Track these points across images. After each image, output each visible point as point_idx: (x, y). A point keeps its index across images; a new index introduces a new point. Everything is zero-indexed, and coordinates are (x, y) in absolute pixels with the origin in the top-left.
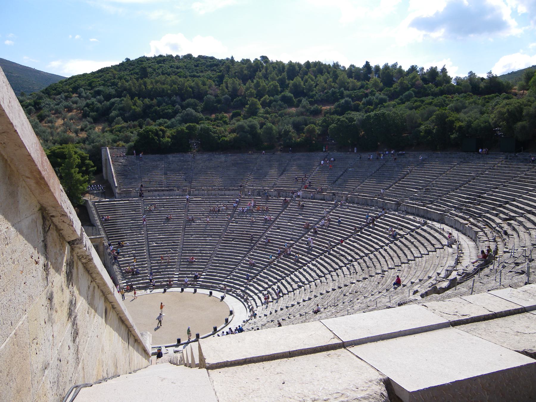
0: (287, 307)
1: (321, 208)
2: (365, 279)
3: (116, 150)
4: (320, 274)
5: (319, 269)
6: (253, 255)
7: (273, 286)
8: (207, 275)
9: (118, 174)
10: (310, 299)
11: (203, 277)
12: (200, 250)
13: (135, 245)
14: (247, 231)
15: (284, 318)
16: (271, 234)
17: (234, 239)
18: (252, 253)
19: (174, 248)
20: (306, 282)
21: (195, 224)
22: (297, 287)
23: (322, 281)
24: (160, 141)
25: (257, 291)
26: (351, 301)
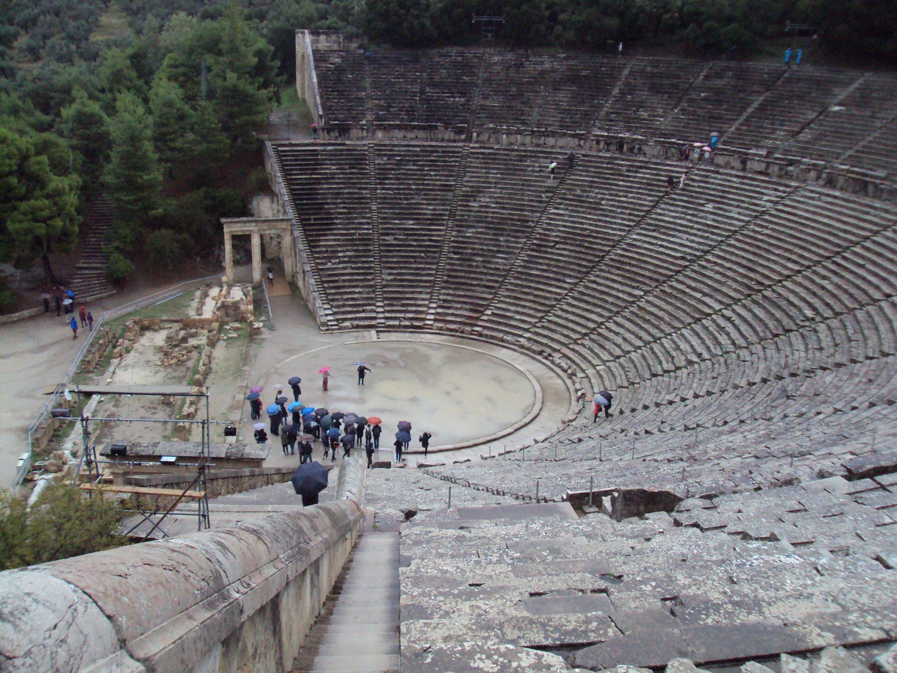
0: (658, 405)
2: (839, 365)
4: (741, 342)
5: (736, 327)
6: (594, 282)
7: (633, 355)
8: (493, 314)
10: (709, 393)
15: (648, 429)
17: (557, 243)
18: (593, 278)
19: (429, 252)
20: (706, 355)
22: (683, 363)
23: (742, 358)
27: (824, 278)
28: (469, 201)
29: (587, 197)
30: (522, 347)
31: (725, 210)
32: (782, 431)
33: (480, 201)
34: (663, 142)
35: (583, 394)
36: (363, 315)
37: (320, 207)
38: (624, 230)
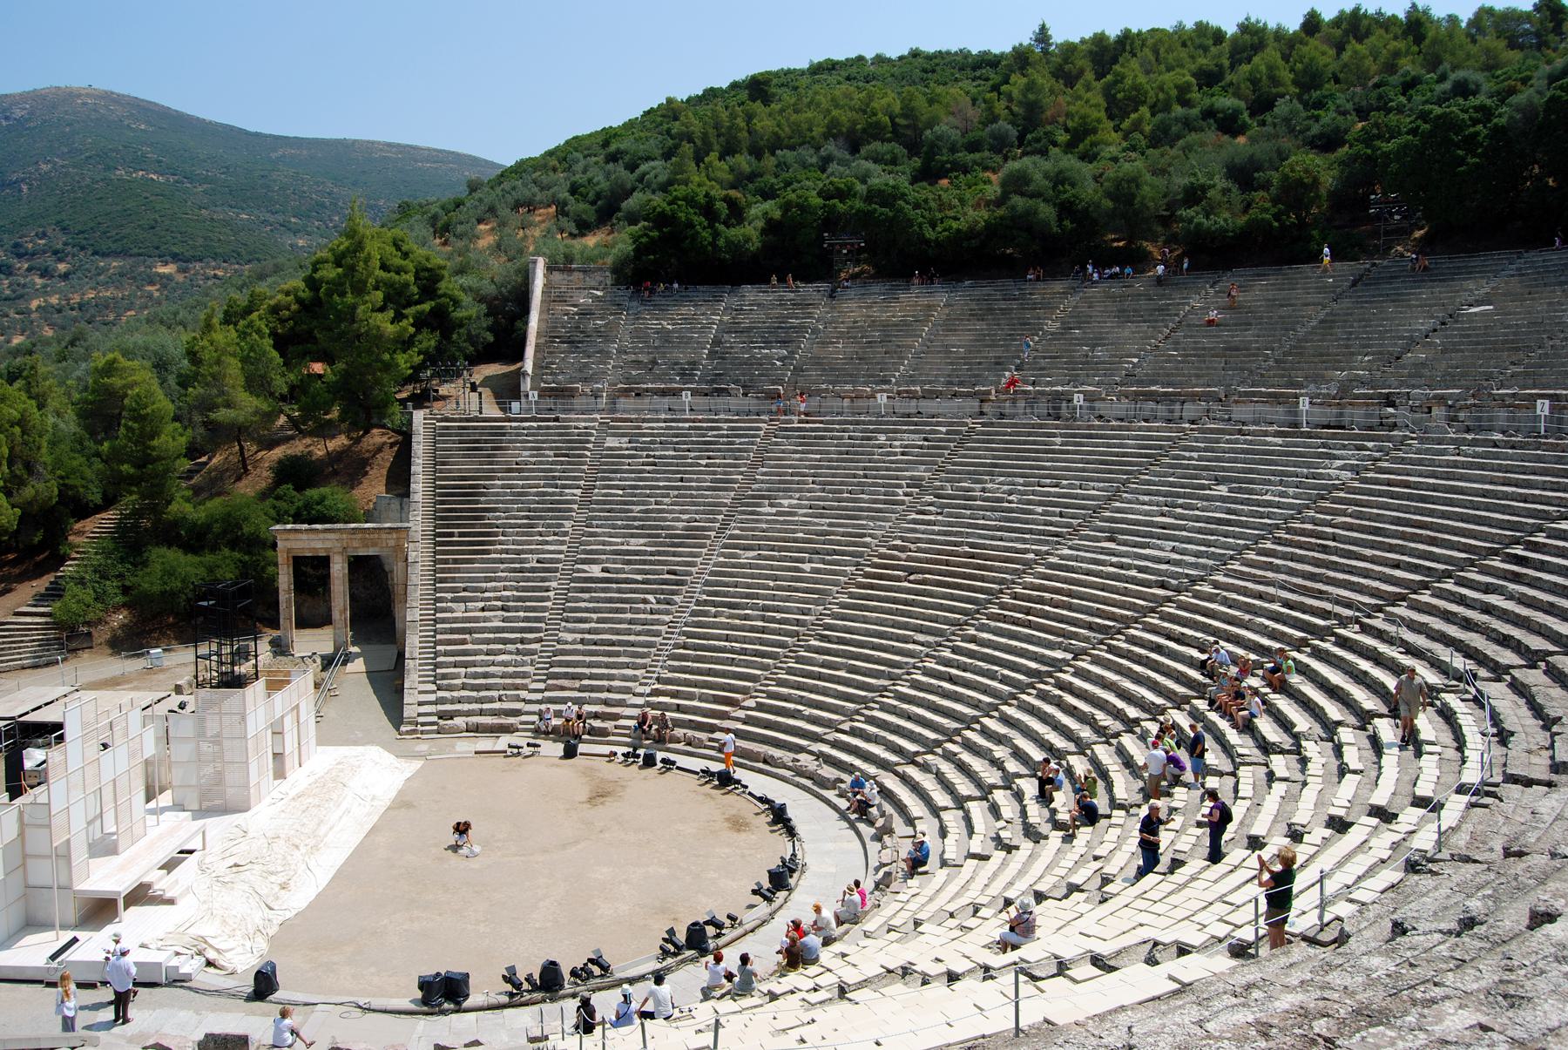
1: (1320, 456)
3: (581, 275)
6: (973, 640)
8: (760, 707)
9: (550, 335)
11: (741, 714)
12: (765, 608)
13: (521, 570)
14: (972, 545)
16: (1076, 559)
17: (912, 571)
18: (972, 631)
19: (663, 592)
21: (774, 510)
24: (716, 234)
25: (941, 798)
26: (1469, 923)
27: (1487, 589)
28: (759, 505)
29: (983, 490)
30: (800, 772)
31: (1251, 492)
32: (1376, 997)
33: (781, 505)
34: (1137, 394)
35: (888, 874)
36: (497, 705)
37: (477, 515)
38: (1046, 543)
